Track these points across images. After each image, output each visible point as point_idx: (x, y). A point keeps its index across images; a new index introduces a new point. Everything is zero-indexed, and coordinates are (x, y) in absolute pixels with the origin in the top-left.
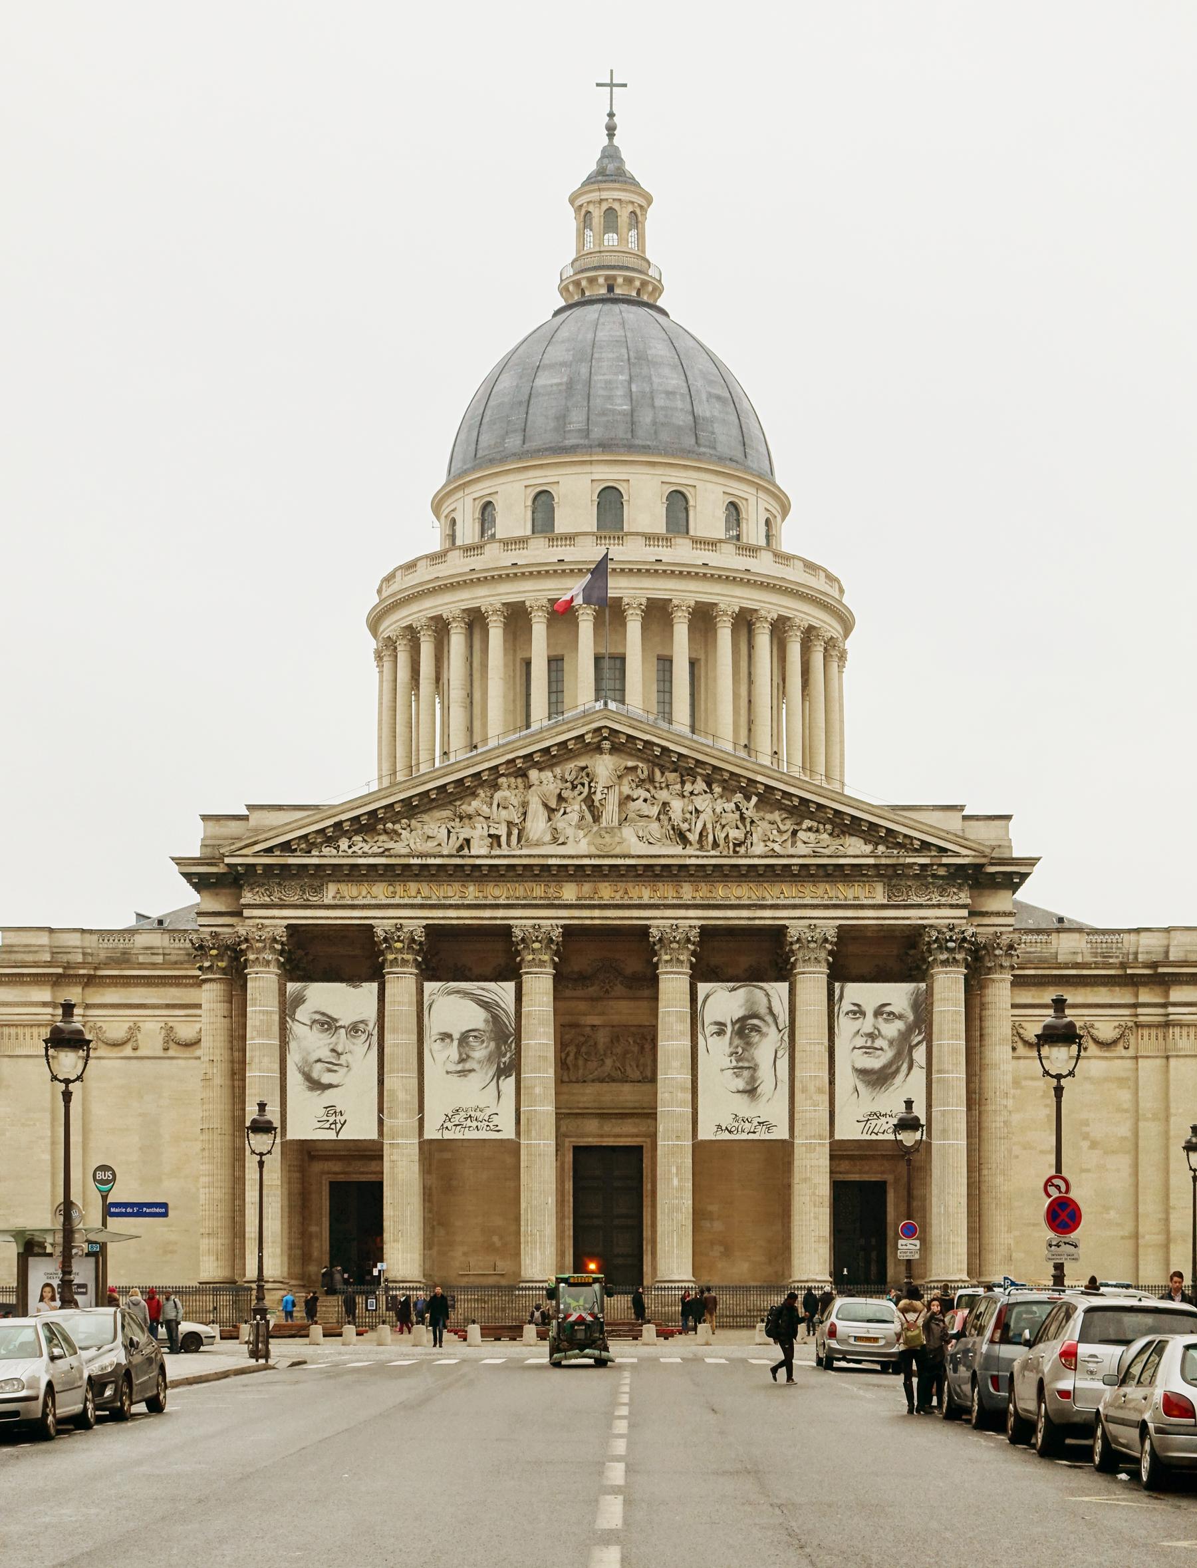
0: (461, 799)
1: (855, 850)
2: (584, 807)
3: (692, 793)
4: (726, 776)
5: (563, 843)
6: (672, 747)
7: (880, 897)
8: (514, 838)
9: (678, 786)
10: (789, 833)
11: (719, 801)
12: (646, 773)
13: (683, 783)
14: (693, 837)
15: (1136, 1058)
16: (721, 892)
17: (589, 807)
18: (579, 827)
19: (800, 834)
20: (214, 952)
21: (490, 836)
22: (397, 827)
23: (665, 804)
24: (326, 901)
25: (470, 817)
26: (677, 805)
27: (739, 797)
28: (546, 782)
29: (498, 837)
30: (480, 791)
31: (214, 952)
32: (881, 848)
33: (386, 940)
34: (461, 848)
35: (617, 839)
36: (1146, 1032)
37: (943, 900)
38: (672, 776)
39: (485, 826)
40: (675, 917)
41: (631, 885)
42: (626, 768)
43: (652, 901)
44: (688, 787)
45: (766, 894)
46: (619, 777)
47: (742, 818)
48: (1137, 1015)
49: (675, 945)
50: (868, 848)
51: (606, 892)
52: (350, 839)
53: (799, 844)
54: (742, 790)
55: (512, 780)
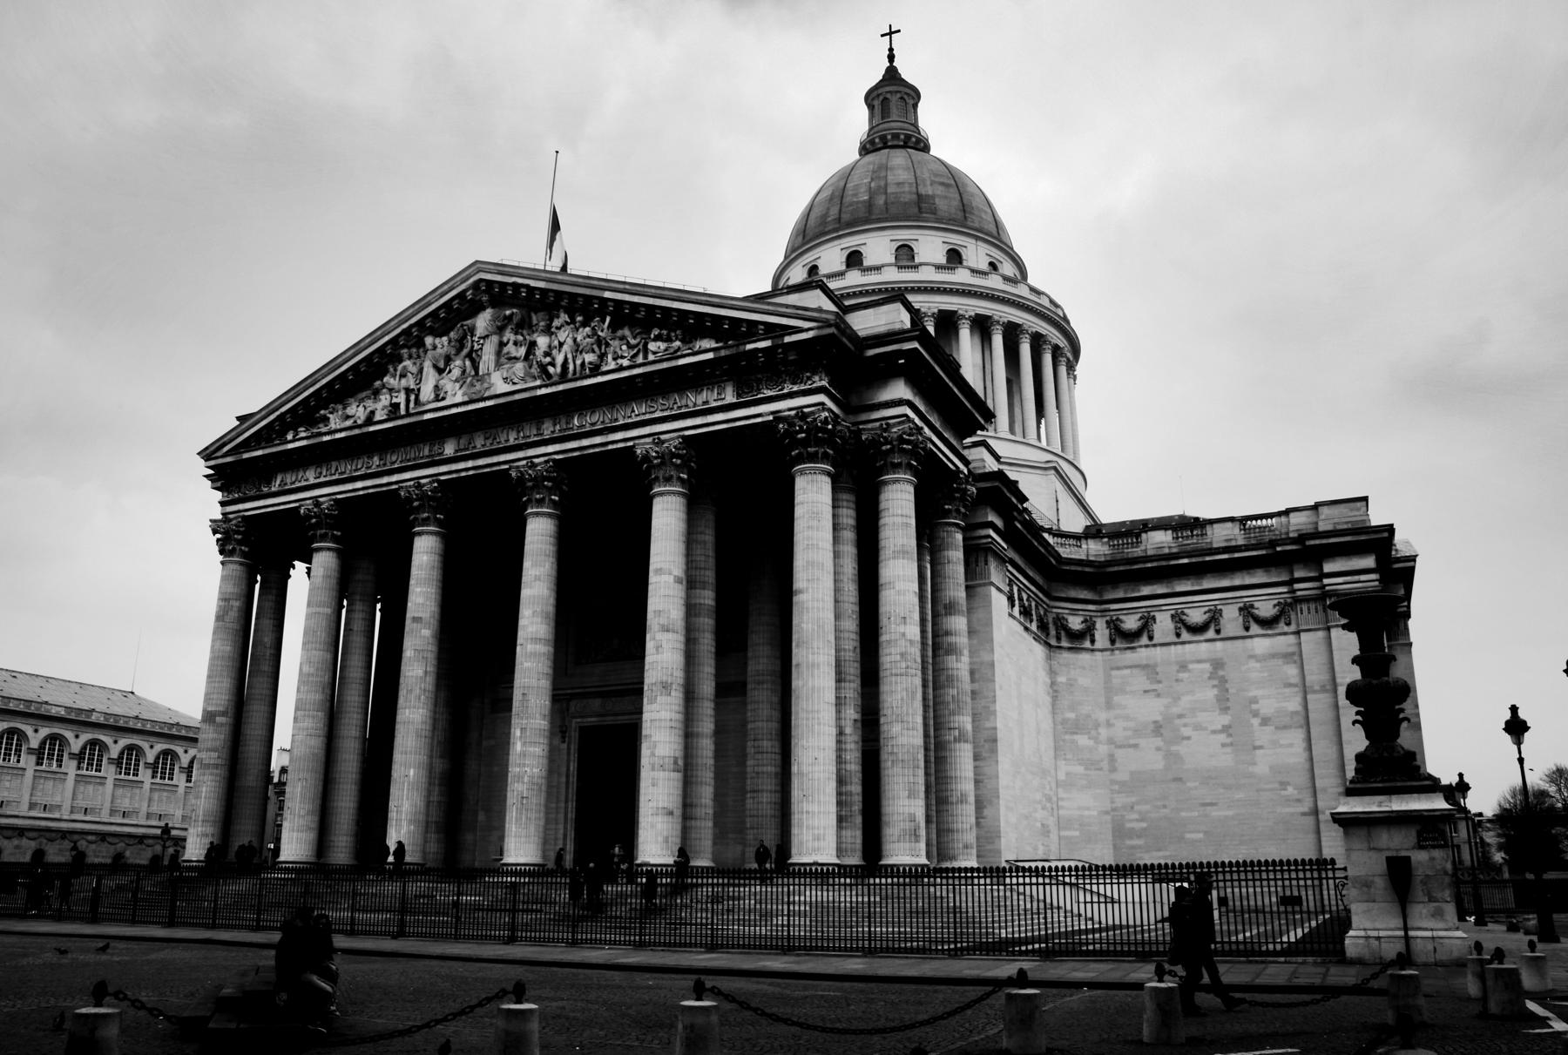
1: (706, 350)
2: (468, 363)
6: (533, 283)
7: (730, 397)
8: (412, 405)
15: (1298, 633)
19: (652, 346)
21: (392, 405)
26: (542, 341)
28: (440, 345)
36: (1305, 607)
37: (795, 388)
38: (541, 315)
42: (505, 317)
44: (556, 323)
47: (599, 342)
48: (1294, 591)
51: (479, 443)
53: (651, 357)
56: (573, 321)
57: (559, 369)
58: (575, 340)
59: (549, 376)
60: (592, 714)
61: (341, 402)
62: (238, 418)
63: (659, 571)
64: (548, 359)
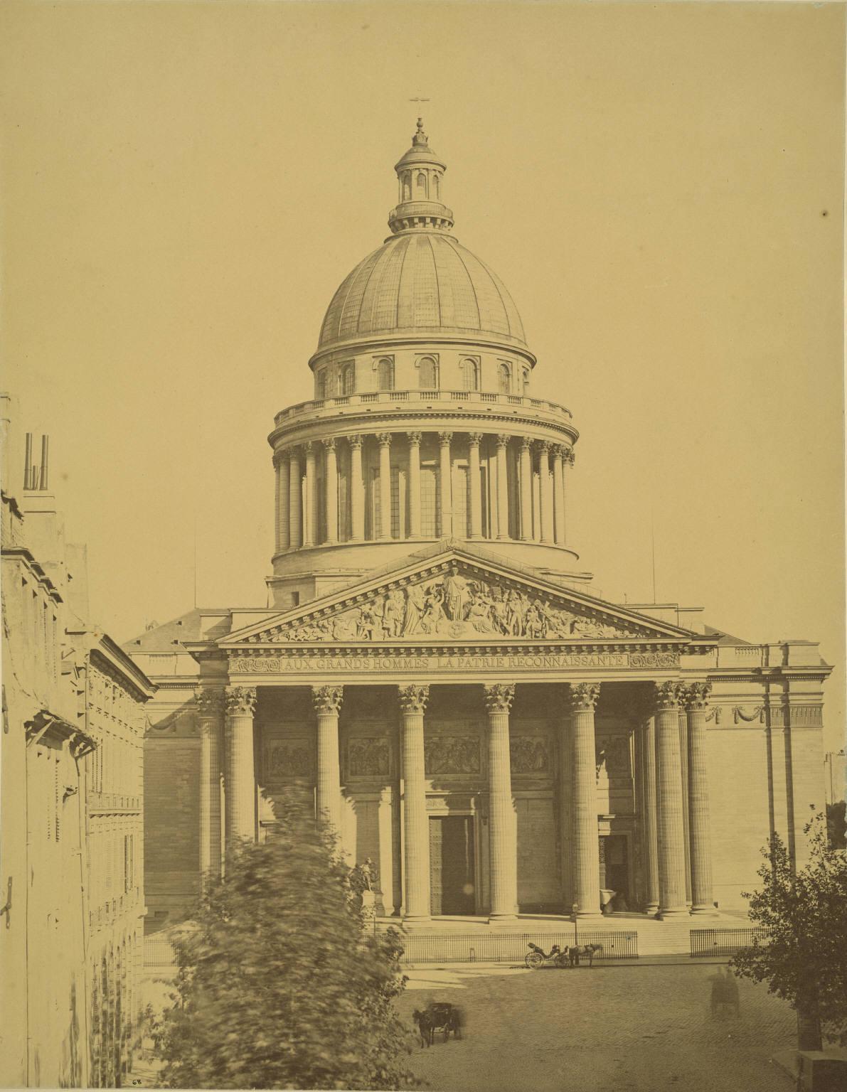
3: (508, 600)
7: (625, 663)
13: (503, 593)
14: (510, 628)
17: (444, 609)
19: (576, 625)
21: (384, 628)
23: (491, 607)
24: (282, 671)
26: (501, 608)
27: (538, 602)
29: (388, 629)
32: (627, 633)
34: (366, 635)
44: (506, 596)
50: (619, 633)
52: (296, 630)
53: (575, 631)
54: (539, 597)
55: (396, 592)
59: (505, 631)
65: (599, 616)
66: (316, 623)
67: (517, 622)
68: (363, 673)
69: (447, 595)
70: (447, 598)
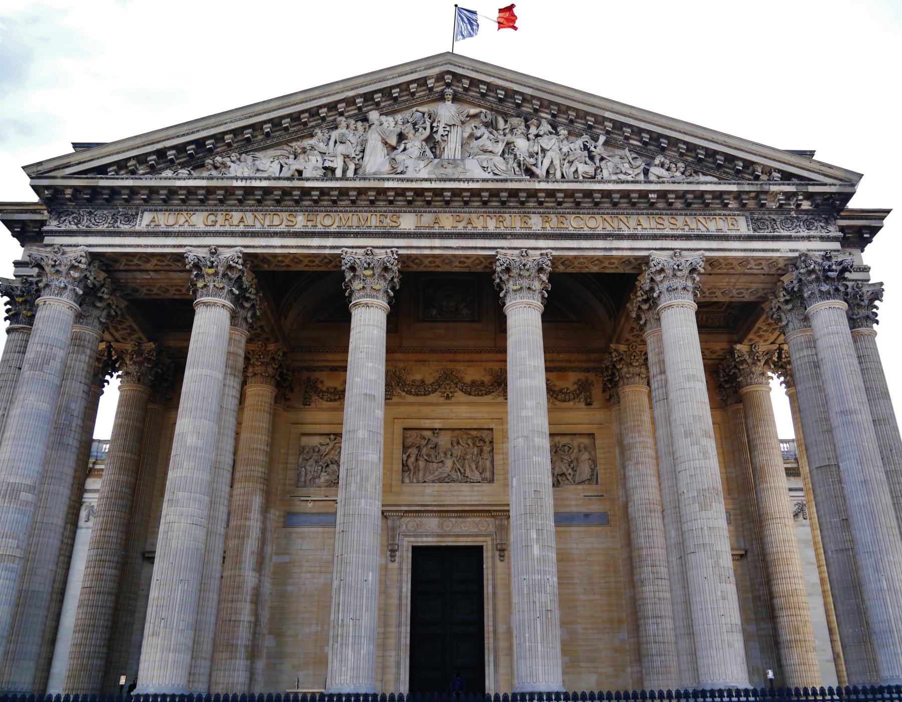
0: (297, 140)
3: (537, 136)
4: (572, 114)
5: (401, 173)
9: (523, 127)
10: (642, 167)
11: (565, 142)
12: (489, 117)
13: (528, 127)
14: (541, 171)
16: (573, 223)
17: (431, 149)
18: (419, 158)
19: (653, 170)
20: (20, 300)
22: (227, 160)
24: (137, 228)
25: (304, 151)
26: (522, 145)
27: (586, 137)
29: (333, 170)
30: (318, 131)
31: (20, 300)
33: (197, 266)
35: (459, 169)
38: (515, 121)
39: (319, 159)
40: (524, 247)
41: (474, 216)
43: (498, 231)
44: (533, 130)
45: (622, 225)
46: (463, 123)
47: (592, 158)
49: (527, 274)
51: (447, 222)
53: (652, 178)
55: (353, 122)
56: (557, 133)
57: (545, 174)
58: (560, 150)
60: (431, 533)
61: (246, 153)
62: (75, 145)
63: (689, 378)
64: (532, 161)
65: (690, 159)
66: (211, 162)
67: (552, 162)
68: (282, 235)
69: (435, 124)
70: (435, 129)
